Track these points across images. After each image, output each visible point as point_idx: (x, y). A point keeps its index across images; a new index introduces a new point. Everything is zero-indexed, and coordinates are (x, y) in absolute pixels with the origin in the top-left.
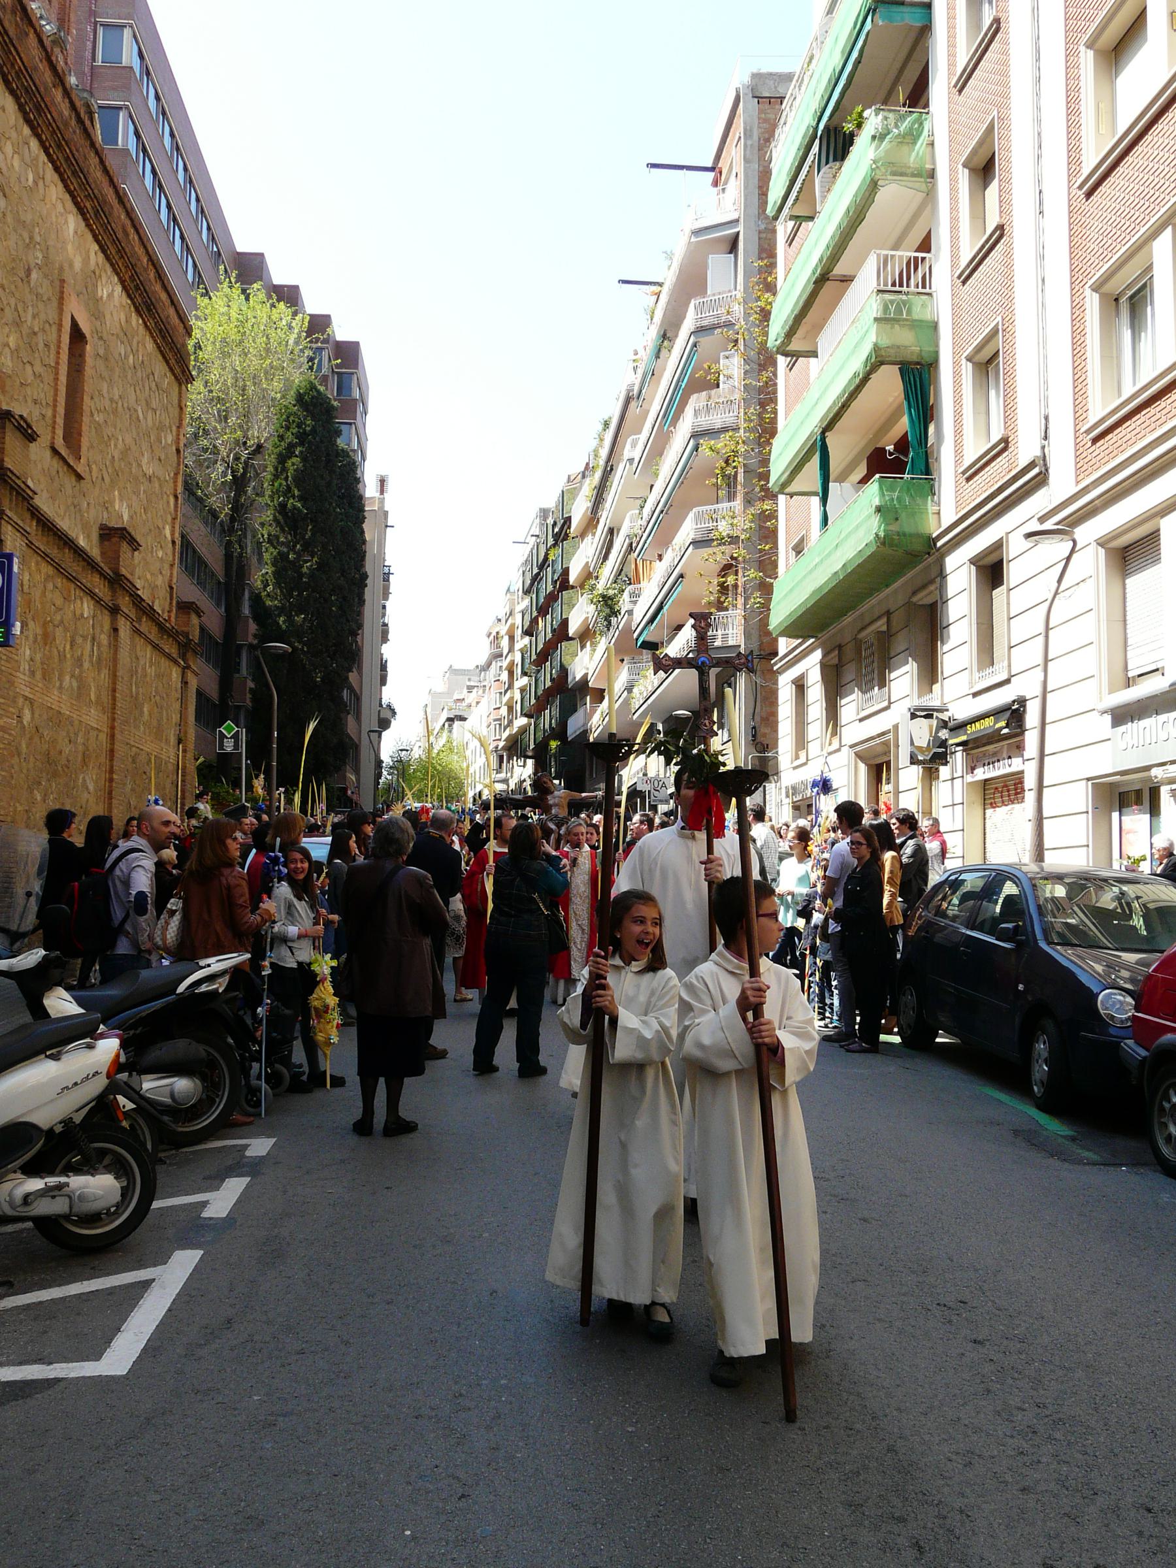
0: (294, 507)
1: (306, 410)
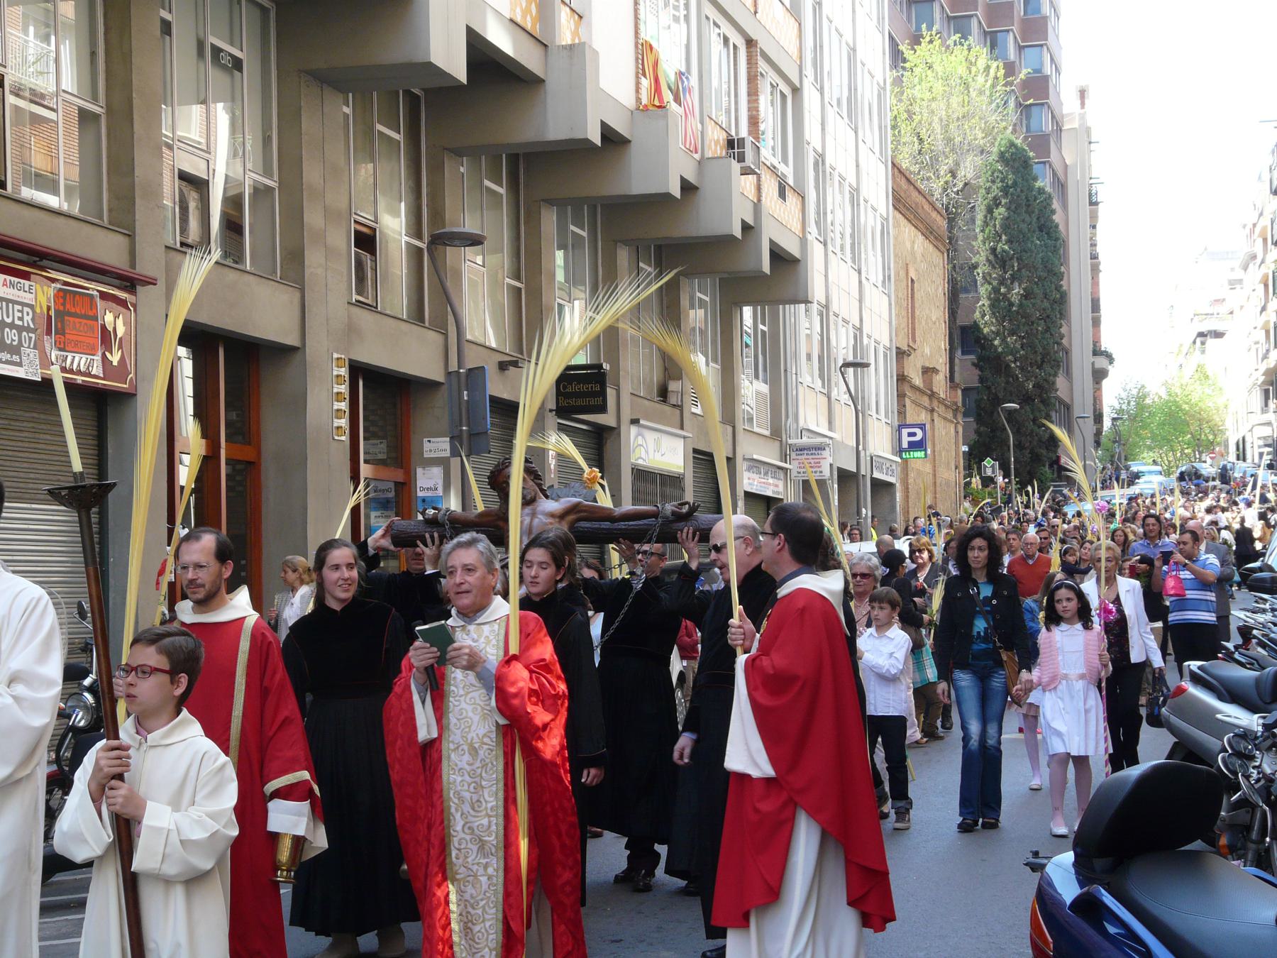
0: (1004, 251)
1: (1007, 165)
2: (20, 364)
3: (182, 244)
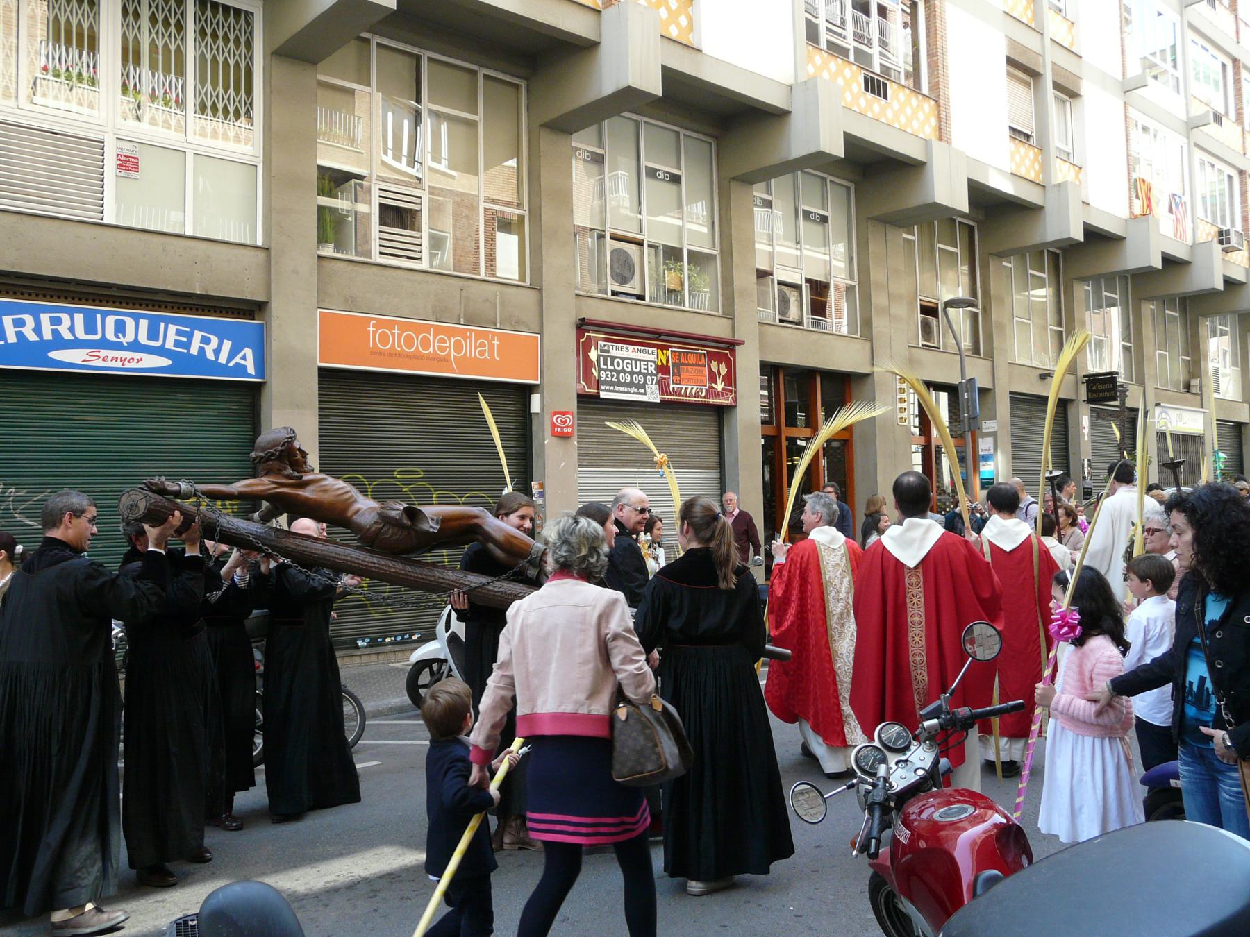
2: (645, 394)
3: (781, 321)
